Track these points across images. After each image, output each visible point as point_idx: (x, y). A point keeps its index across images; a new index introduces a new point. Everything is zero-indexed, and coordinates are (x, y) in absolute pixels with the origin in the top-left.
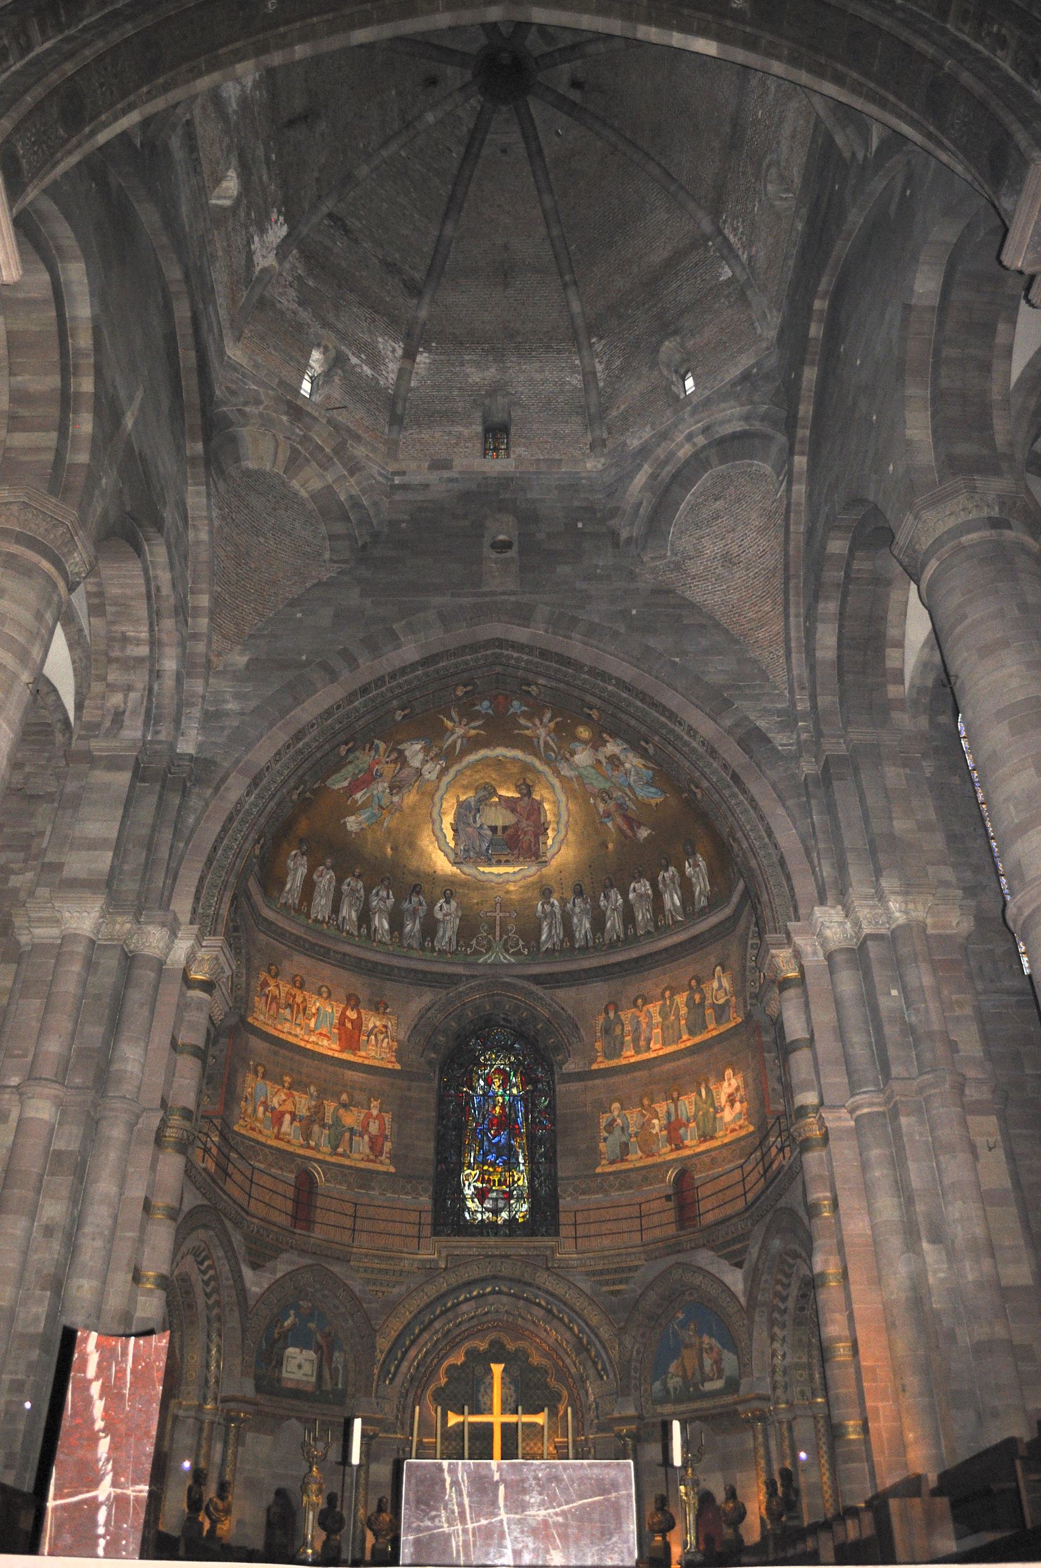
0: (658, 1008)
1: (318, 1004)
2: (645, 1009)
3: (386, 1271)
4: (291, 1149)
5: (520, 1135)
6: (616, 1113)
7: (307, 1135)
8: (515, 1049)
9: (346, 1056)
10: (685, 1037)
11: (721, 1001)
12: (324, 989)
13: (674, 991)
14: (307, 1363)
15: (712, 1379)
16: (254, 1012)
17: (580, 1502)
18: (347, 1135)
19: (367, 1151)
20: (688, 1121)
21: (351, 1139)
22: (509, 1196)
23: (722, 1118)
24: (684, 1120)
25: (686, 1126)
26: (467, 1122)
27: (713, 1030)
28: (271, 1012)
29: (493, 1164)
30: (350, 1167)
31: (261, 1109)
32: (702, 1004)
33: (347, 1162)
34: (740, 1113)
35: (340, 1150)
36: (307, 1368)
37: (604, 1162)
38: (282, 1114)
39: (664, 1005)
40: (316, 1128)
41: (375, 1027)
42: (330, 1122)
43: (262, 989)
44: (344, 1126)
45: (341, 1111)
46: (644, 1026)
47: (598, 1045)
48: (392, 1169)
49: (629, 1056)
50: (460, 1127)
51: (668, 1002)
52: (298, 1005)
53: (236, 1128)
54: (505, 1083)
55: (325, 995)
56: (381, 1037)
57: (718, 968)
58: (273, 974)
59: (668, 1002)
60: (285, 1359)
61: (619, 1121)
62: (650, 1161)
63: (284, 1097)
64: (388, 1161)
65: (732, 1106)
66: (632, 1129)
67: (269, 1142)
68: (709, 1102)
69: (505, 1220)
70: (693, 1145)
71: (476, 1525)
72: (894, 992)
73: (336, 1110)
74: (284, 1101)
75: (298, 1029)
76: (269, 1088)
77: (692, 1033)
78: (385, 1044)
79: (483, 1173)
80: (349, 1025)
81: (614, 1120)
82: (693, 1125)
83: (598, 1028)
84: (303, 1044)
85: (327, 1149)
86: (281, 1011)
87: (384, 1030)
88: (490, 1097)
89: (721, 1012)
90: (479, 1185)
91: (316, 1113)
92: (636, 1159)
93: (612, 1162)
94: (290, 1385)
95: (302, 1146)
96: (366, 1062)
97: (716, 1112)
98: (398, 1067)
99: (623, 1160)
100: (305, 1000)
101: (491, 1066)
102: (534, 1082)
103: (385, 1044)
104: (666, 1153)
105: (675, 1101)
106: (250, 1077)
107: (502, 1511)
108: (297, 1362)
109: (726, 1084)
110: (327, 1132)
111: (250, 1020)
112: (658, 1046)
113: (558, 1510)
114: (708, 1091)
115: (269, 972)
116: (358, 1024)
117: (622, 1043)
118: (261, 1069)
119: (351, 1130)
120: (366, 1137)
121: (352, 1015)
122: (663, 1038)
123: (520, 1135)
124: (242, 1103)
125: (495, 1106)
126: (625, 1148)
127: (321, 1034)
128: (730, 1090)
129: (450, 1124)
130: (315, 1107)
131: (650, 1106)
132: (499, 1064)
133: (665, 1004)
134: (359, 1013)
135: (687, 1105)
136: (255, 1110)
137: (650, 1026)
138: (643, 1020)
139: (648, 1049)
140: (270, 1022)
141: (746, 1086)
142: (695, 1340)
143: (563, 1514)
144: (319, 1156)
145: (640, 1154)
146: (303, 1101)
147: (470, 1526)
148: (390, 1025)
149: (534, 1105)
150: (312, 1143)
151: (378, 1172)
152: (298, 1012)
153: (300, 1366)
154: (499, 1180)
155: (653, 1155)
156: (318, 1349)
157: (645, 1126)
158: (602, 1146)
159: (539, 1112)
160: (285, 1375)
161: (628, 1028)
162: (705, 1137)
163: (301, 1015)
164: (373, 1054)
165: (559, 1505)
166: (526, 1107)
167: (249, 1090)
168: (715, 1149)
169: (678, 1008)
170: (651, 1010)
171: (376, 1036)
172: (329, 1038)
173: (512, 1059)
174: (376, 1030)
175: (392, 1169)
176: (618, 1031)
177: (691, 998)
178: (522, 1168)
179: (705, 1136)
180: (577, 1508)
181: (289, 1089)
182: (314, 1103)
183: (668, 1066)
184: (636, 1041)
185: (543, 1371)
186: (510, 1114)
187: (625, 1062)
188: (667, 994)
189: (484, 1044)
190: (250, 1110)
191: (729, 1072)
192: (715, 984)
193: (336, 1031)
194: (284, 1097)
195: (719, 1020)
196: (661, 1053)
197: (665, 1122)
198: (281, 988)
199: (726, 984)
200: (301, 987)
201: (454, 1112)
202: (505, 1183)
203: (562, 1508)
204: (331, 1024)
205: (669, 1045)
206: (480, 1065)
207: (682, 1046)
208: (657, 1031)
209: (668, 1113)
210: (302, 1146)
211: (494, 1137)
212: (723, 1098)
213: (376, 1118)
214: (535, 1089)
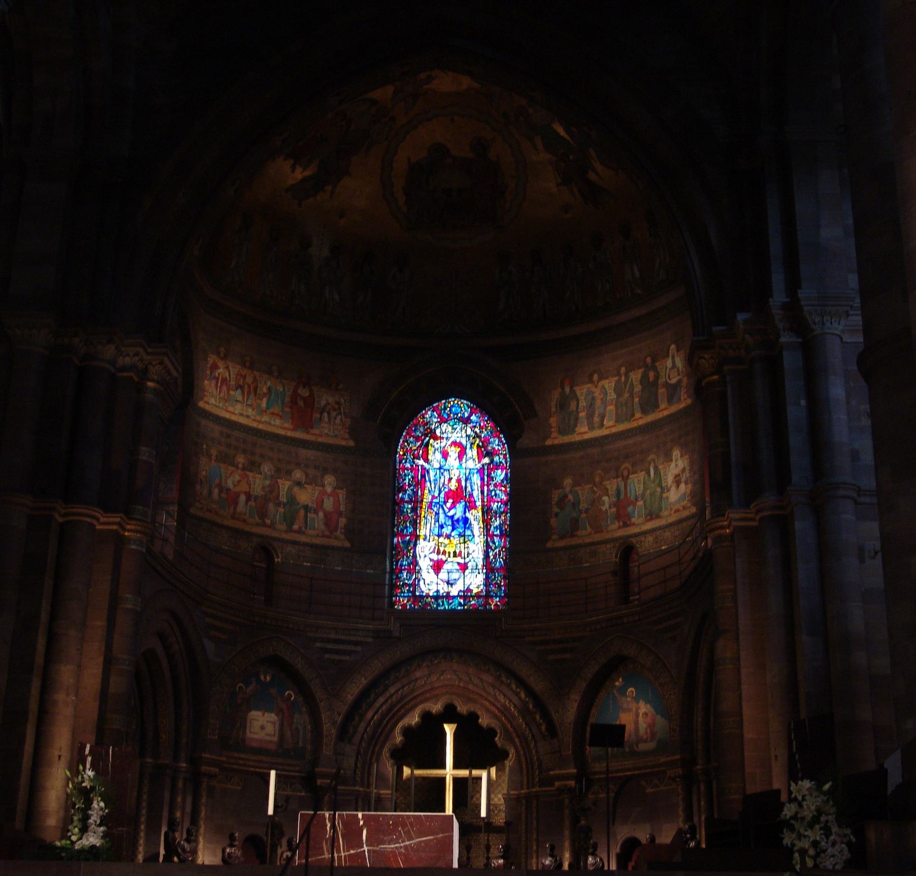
0: (613, 385)
1: (269, 383)
2: (600, 384)
3: (342, 642)
4: (247, 529)
5: (475, 507)
6: (568, 490)
7: (263, 514)
8: (471, 422)
9: (299, 435)
10: (638, 415)
11: (674, 381)
12: (274, 368)
13: (631, 368)
14: (269, 724)
15: (646, 741)
16: (205, 396)
17: (418, 840)
18: (302, 513)
19: (323, 527)
20: (637, 500)
21: (306, 516)
22: (463, 567)
23: (667, 498)
24: (632, 498)
25: (634, 504)
26: (423, 495)
27: (665, 410)
28: (222, 395)
29: (448, 537)
30: (305, 545)
31: (216, 491)
32: (655, 383)
33: (303, 539)
34: (684, 494)
35: (296, 527)
36: (270, 729)
37: (554, 537)
38: (237, 495)
39: (618, 382)
40: (271, 506)
41: (328, 404)
42: (285, 501)
43: (211, 374)
44: (299, 504)
45: (296, 489)
46: (598, 402)
47: (553, 421)
48: (347, 544)
49: (584, 432)
50: (416, 502)
51: (623, 378)
52: (249, 386)
53: (192, 511)
54: (462, 454)
55: (276, 374)
56: (334, 414)
57: (673, 347)
58: (222, 355)
59: (623, 378)
60: (248, 721)
61: (570, 497)
62: (598, 537)
63: (237, 477)
64: (342, 537)
65: (678, 486)
66: (583, 506)
67: (226, 523)
68: (657, 481)
69: (460, 591)
70: (640, 524)
71: (347, 853)
72: (803, 402)
73: (290, 489)
74: (239, 482)
75: (250, 410)
76: (223, 471)
77: (645, 412)
78: (338, 421)
79: (439, 544)
80: (301, 403)
81: (566, 496)
82: (640, 503)
83: (553, 403)
84: (255, 425)
85: (283, 527)
86: (232, 393)
87: (337, 406)
88: (445, 470)
89: (673, 391)
90: (435, 557)
91: (271, 492)
92: (585, 535)
93: (562, 537)
94: (254, 744)
95: (258, 524)
96: (320, 440)
97: (662, 492)
98: (351, 443)
99: (573, 536)
100: (255, 380)
101: (447, 438)
102: (491, 454)
103: (338, 421)
104: (616, 531)
105: (625, 479)
106: (203, 461)
107: (365, 845)
108: (260, 723)
109: (673, 465)
110: (281, 510)
111: (201, 404)
112: (611, 423)
113: (402, 845)
114: (656, 469)
115: (218, 354)
116: (310, 402)
117: (577, 419)
118: (214, 452)
119: (306, 508)
120: (321, 514)
121: (304, 392)
122: (617, 414)
123: (475, 507)
124: (198, 487)
125: (450, 479)
126: (575, 524)
127: (273, 414)
128: (676, 471)
129: (406, 498)
130: (270, 486)
131: (601, 483)
132: (455, 437)
133: (620, 379)
134: (311, 391)
135: (637, 483)
136: (210, 493)
137: (605, 403)
138: (597, 393)
139: (602, 425)
140: (221, 405)
141: (691, 469)
142: (633, 706)
143: (406, 847)
144: (275, 534)
145: (589, 529)
146: (257, 481)
147: (343, 854)
148: (342, 401)
149: (490, 478)
150: (268, 521)
151: (333, 548)
152: (249, 393)
153: (262, 728)
154: (455, 553)
155: (602, 531)
156: (280, 712)
157: (595, 502)
158: (553, 522)
159: (495, 485)
160: (249, 735)
161: (583, 404)
162: (652, 515)
163: (252, 396)
164: (326, 431)
165: (403, 842)
166: (482, 479)
167: (204, 473)
168: (660, 528)
169: (632, 385)
170: (606, 386)
171: (329, 413)
172: (281, 417)
173: (469, 432)
174: (329, 407)
175: (347, 544)
176: (573, 406)
177: (645, 376)
178: (477, 539)
179: (652, 515)
180: (415, 844)
181: (243, 469)
182: (268, 482)
183: (621, 444)
184: (590, 417)
185: (492, 732)
186: (466, 487)
187: (578, 438)
188: (623, 370)
189: (440, 416)
190: (205, 492)
191: (676, 453)
192: (669, 363)
193: (288, 410)
194: (237, 477)
195: (670, 400)
196: (614, 430)
197: (615, 499)
198: (227, 370)
199: (679, 363)
200: (251, 368)
201: (410, 485)
202: (460, 555)
203: (405, 843)
204: (283, 403)
205: (622, 422)
206: (436, 438)
207: (634, 424)
208: (611, 408)
209: (618, 491)
210: (258, 524)
211: (450, 509)
212: (670, 479)
213: (329, 495)
214: (492, 461)
